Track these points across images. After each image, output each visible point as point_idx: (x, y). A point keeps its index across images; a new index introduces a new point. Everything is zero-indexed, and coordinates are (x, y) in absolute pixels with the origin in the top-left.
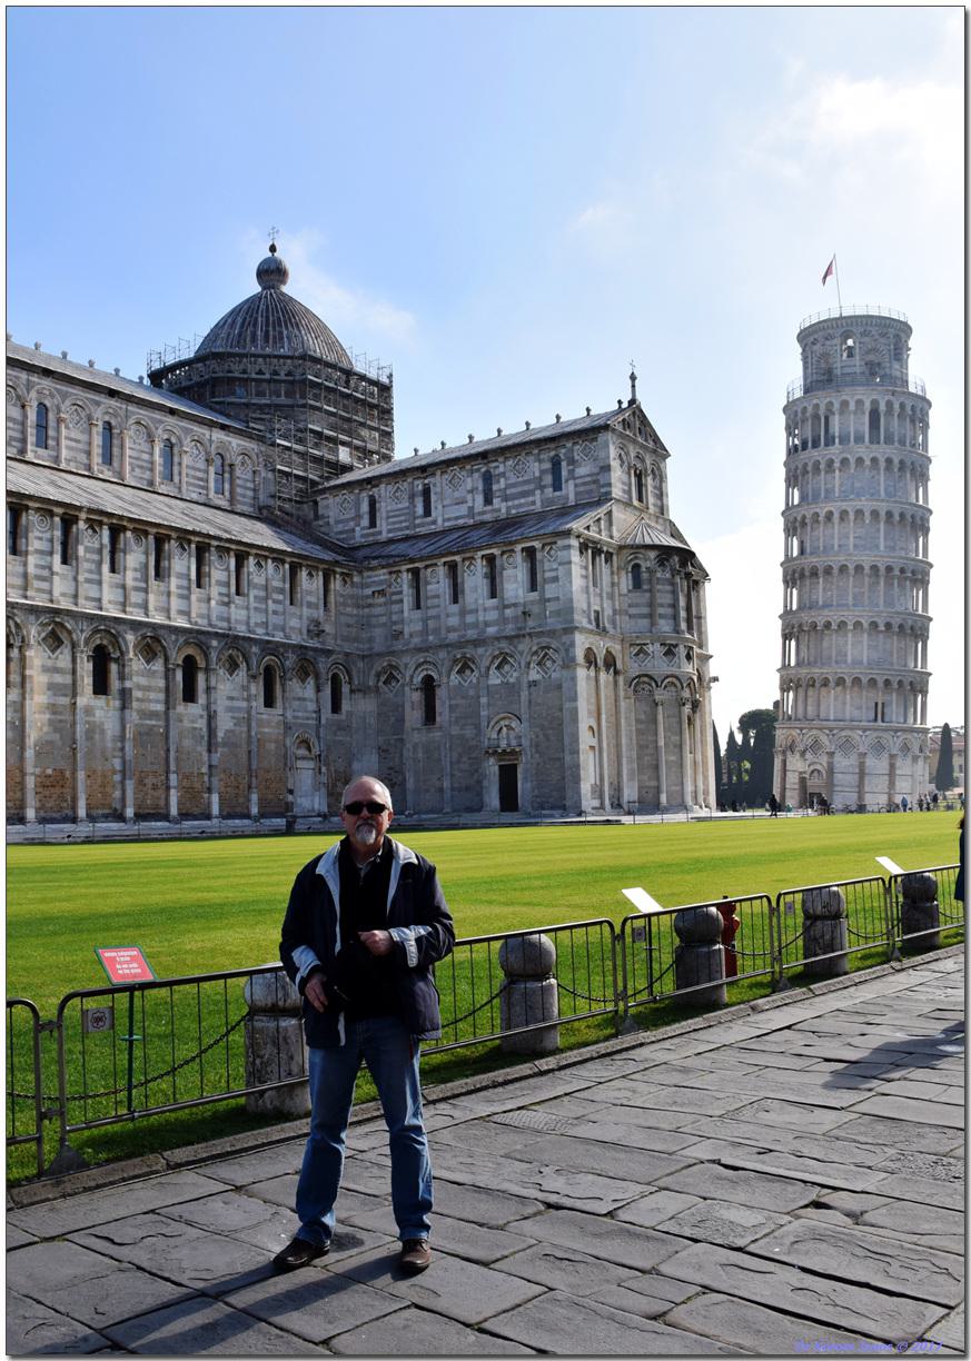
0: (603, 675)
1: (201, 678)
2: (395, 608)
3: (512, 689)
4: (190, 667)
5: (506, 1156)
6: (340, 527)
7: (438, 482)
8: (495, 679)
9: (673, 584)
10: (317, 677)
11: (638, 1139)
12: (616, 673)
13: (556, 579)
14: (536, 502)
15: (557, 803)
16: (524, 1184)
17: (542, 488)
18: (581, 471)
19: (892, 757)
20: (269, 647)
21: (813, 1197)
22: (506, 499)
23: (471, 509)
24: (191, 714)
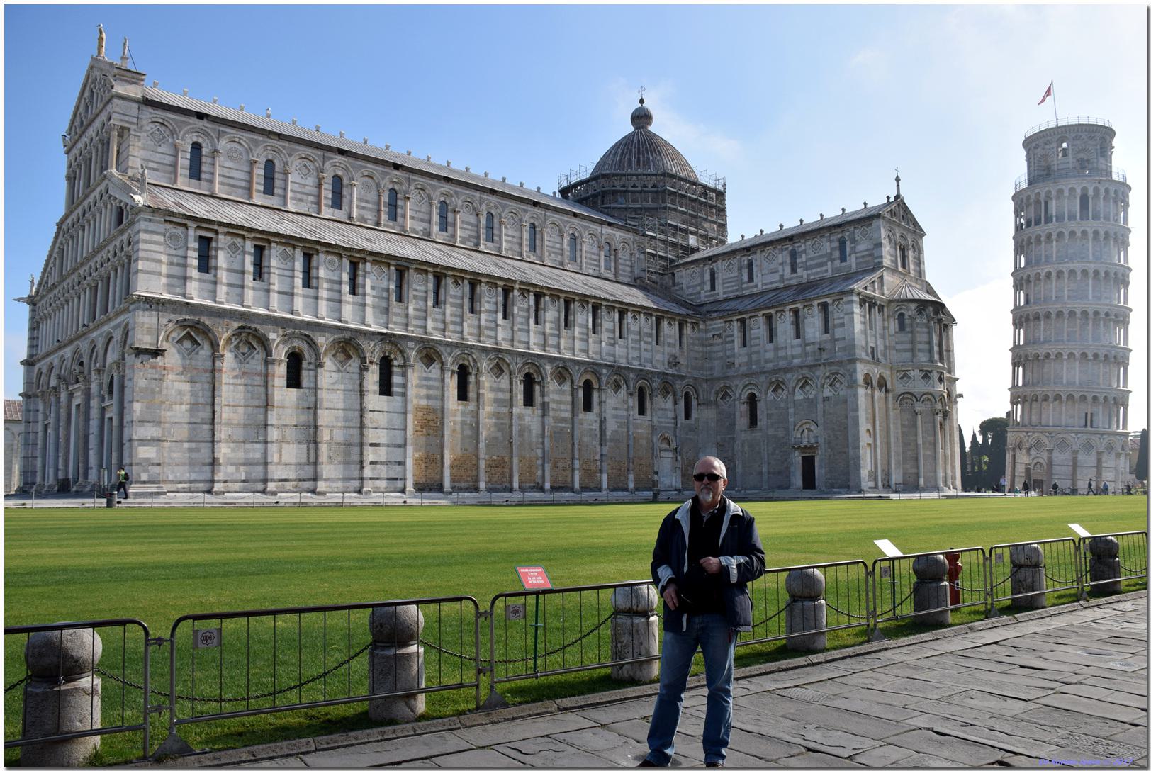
0: (877, 393)
1: (595, 395)
2: (729, 346)
3: (811, 403)
4: (588, 387)
5: (783, 716)
6: (690, 291)
7: (758, 258)
8: (799, 396)
9: (928, 327)
10: (675, 394)
11: (876, 711)
12: (887, 391)
13: (842, 325)
14: (829, 270)
15: (844, 483)
16: (793, 735)
17: (832, 260)
18: (860, 247)
19: (1099, 454)
20: (641, 374)
21: (999, 758)
22: (806, 269)
23: (782, 276)
24: (589, 420)
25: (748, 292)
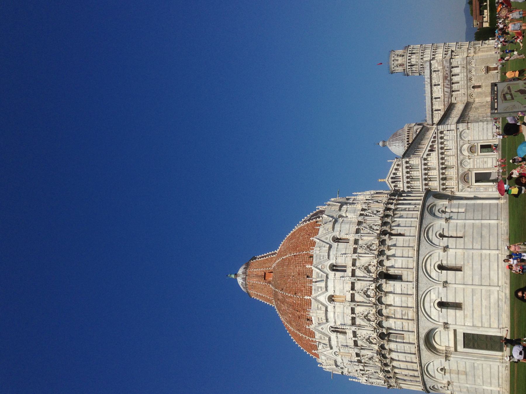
8: (474, 73)
25: (443, 98)
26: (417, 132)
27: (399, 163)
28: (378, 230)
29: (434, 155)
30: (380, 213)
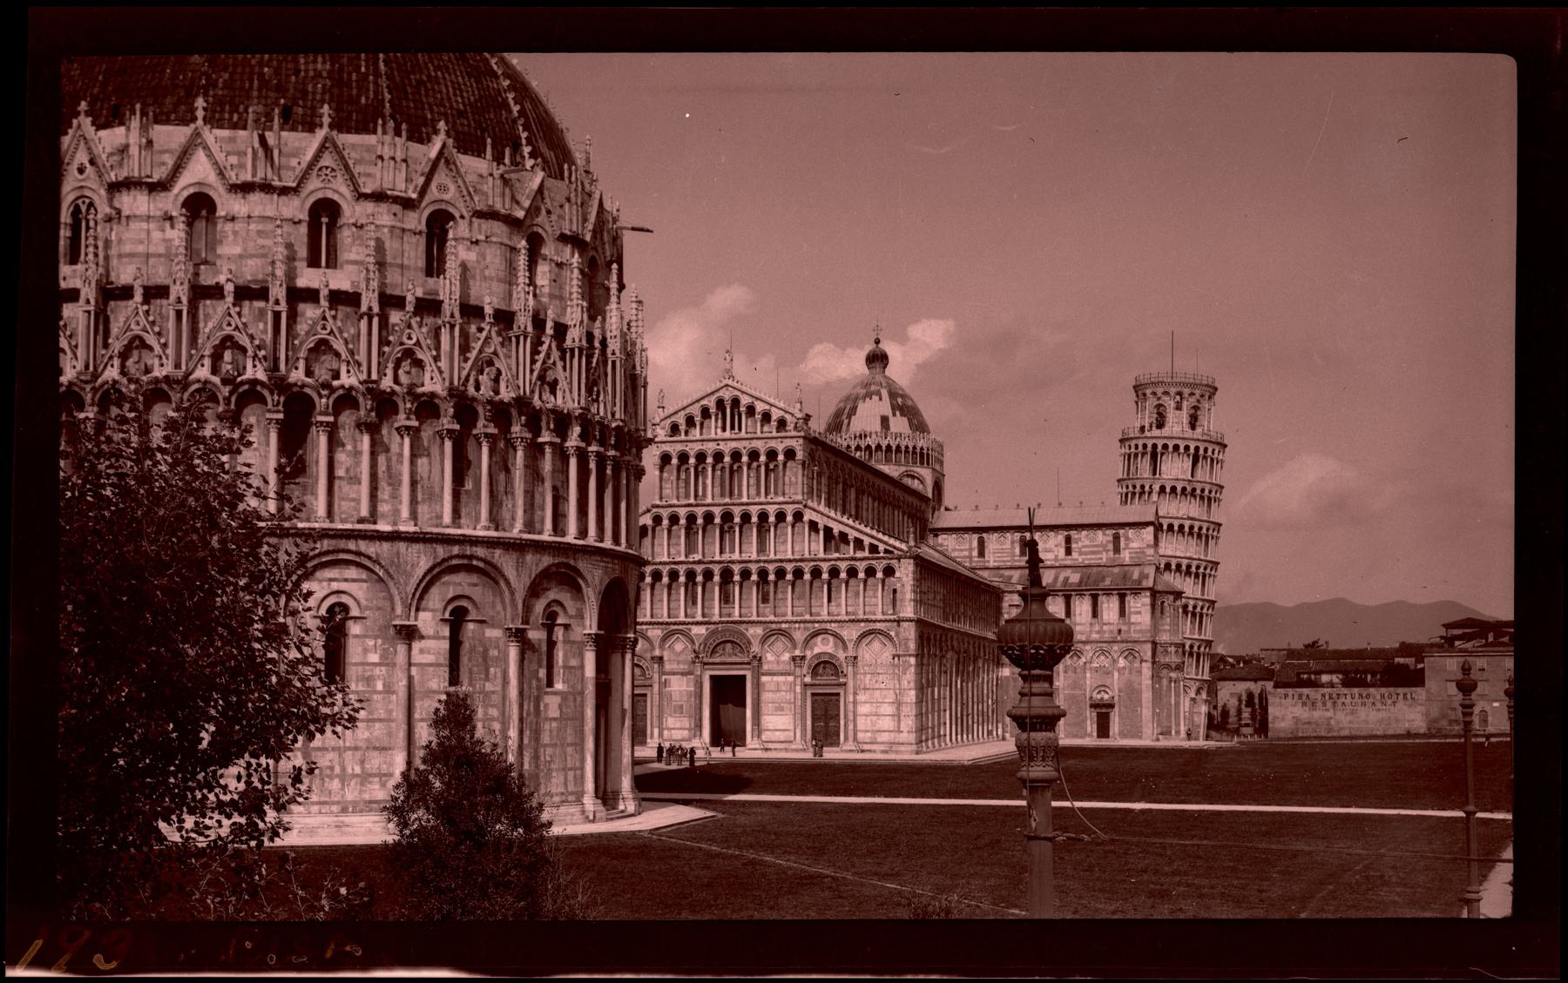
18: (1134, 545)
22: (1081, 553)
26: (908, 482)
27: (790, 427)
28: (477, 388)
29: (816, 546)
30: (547, 396)
